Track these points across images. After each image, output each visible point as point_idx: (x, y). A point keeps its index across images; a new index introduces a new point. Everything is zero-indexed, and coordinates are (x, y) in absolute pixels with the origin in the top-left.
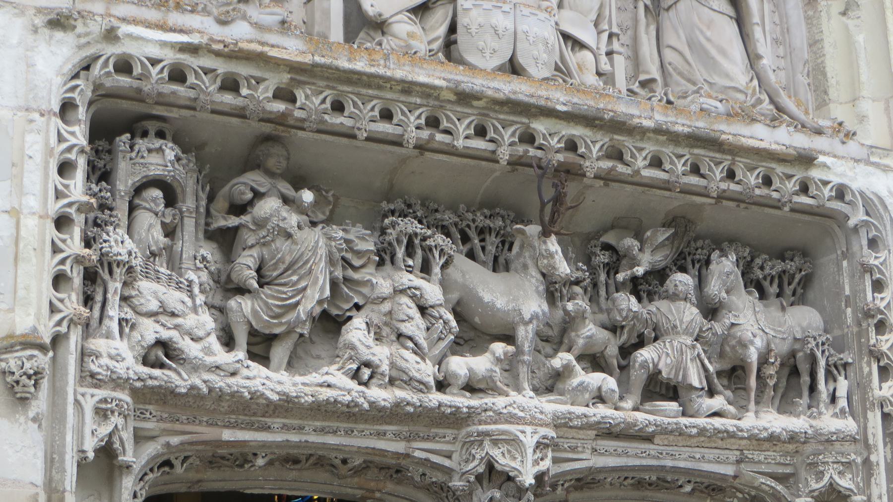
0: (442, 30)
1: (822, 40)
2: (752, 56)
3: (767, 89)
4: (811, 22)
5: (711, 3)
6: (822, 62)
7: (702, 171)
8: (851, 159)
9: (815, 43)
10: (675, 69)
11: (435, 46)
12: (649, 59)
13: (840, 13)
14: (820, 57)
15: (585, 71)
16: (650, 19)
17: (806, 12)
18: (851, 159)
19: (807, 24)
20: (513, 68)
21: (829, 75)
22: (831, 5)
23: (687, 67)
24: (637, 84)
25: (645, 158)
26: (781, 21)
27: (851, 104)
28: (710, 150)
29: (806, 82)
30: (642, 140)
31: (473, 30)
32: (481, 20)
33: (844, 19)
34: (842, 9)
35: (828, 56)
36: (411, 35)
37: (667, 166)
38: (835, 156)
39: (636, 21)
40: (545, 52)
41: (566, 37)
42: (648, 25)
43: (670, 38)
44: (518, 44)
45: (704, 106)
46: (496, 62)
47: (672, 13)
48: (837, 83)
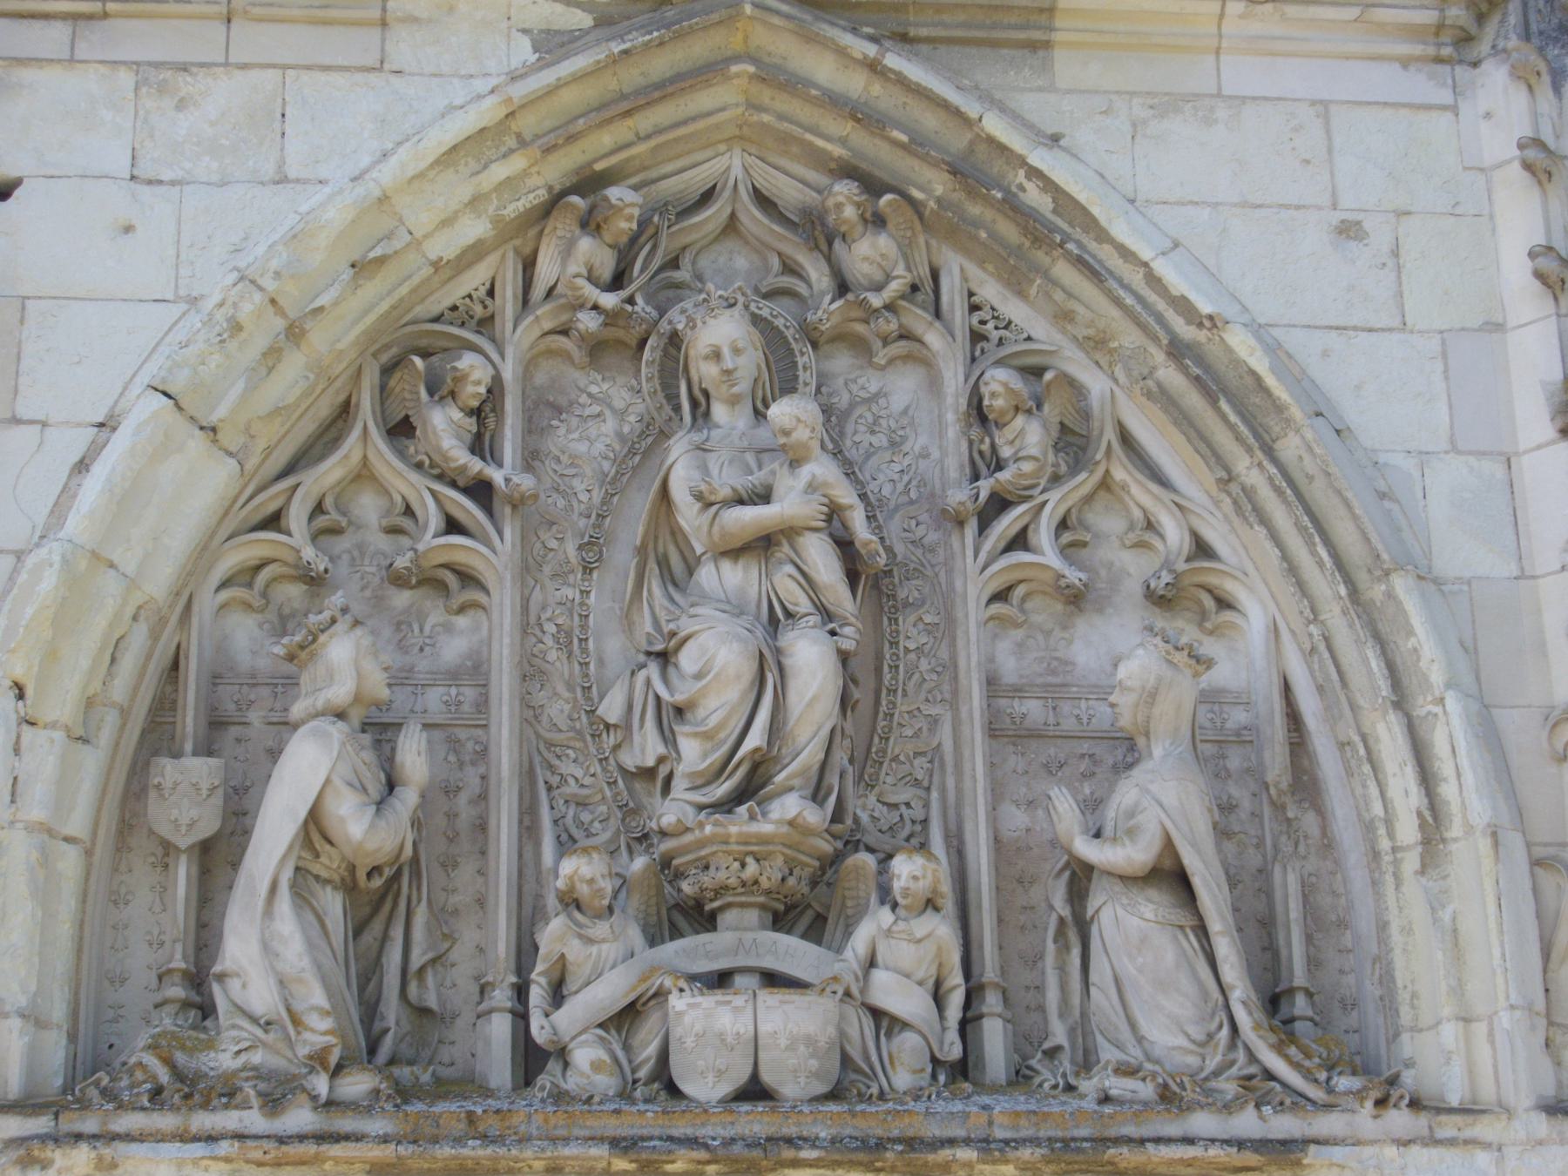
0: (652, 1049)
5: (1142, 909)
11: (642, 1074)
13: (1416, 873)
15: (899, 1069)
20: (755, 1091)
21: (1400, 983)
22: (1402, 859)
24: (1039, 1055)
29: (1378, 993)
31: (689, 1042)
32: (698, 1028)
33: (1423, 880)
34: (1417, 865)
36: (597, 1066)
40: (812, 1056)
41: (877, 1014)
44: (762, 1055)
45: (1113, 1092)
46: (726, 1088)
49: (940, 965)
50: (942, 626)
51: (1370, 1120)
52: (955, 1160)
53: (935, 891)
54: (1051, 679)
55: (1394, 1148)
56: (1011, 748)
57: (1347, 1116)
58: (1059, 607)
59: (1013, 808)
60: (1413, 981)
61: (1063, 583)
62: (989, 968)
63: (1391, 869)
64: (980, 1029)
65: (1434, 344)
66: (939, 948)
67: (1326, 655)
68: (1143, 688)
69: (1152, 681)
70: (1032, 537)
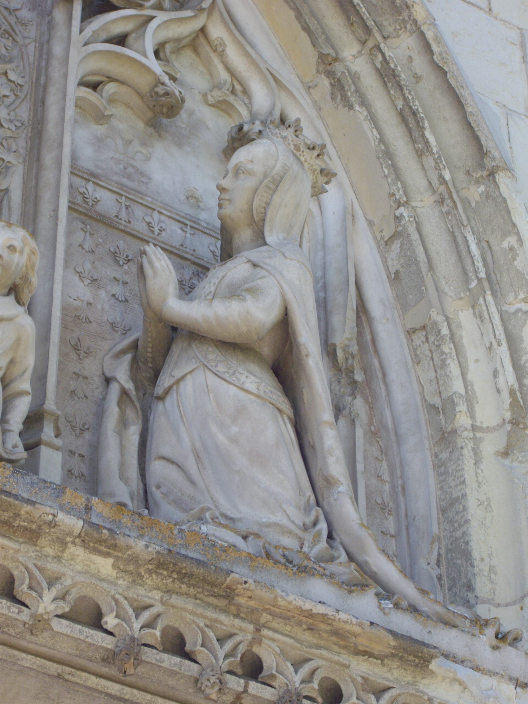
1: (464, 496)
2: (319, 482)
3: (347, 540)
4: (445, 468)
5: (243, 378)
6: (464, 534)
7: (188, 648)
8: (511, 679)
9: (451, 507)
10: (165, 495)
12: (116, 472)
14: (460, 526)
16: (130, 414)
17: (436, 456)
18: (511, 679)
19: (439, 474)
21: (475, 554)
22: (481, 439)
23: (188, 489)
25: (62, 597)
26: (392, 473)
27: (517, 607)
28: (209, 605)
29: (435, 573)
30: (58, 558)
33: (507, 462)
34: (501, 446)
35: (474, 524)
37: (110, 621)
38: (477, 669)
39: (100, 414)
42: (123, 423)
43: (163, 443)
47: (169, 401)
48: (492, 569)
49: (12, 362)
50: (25, 88)
51: (489, 650)
52: (53, 524)
53: (25, 279)
54: (125, 181)
55: (513, 687)
56: (81, 226)
57: (467, 638)
58: (141, 125)
59: (76, 278)
60: (490, 556)
61: (160, 90)
62: (50, 404)
63: (471, 445)
64: (39, 450)
65: (515, 35)
66: (18, 341)
67: (415, 236)
68: (266, 175)
69: (278, 168)
70: (131, 40)
